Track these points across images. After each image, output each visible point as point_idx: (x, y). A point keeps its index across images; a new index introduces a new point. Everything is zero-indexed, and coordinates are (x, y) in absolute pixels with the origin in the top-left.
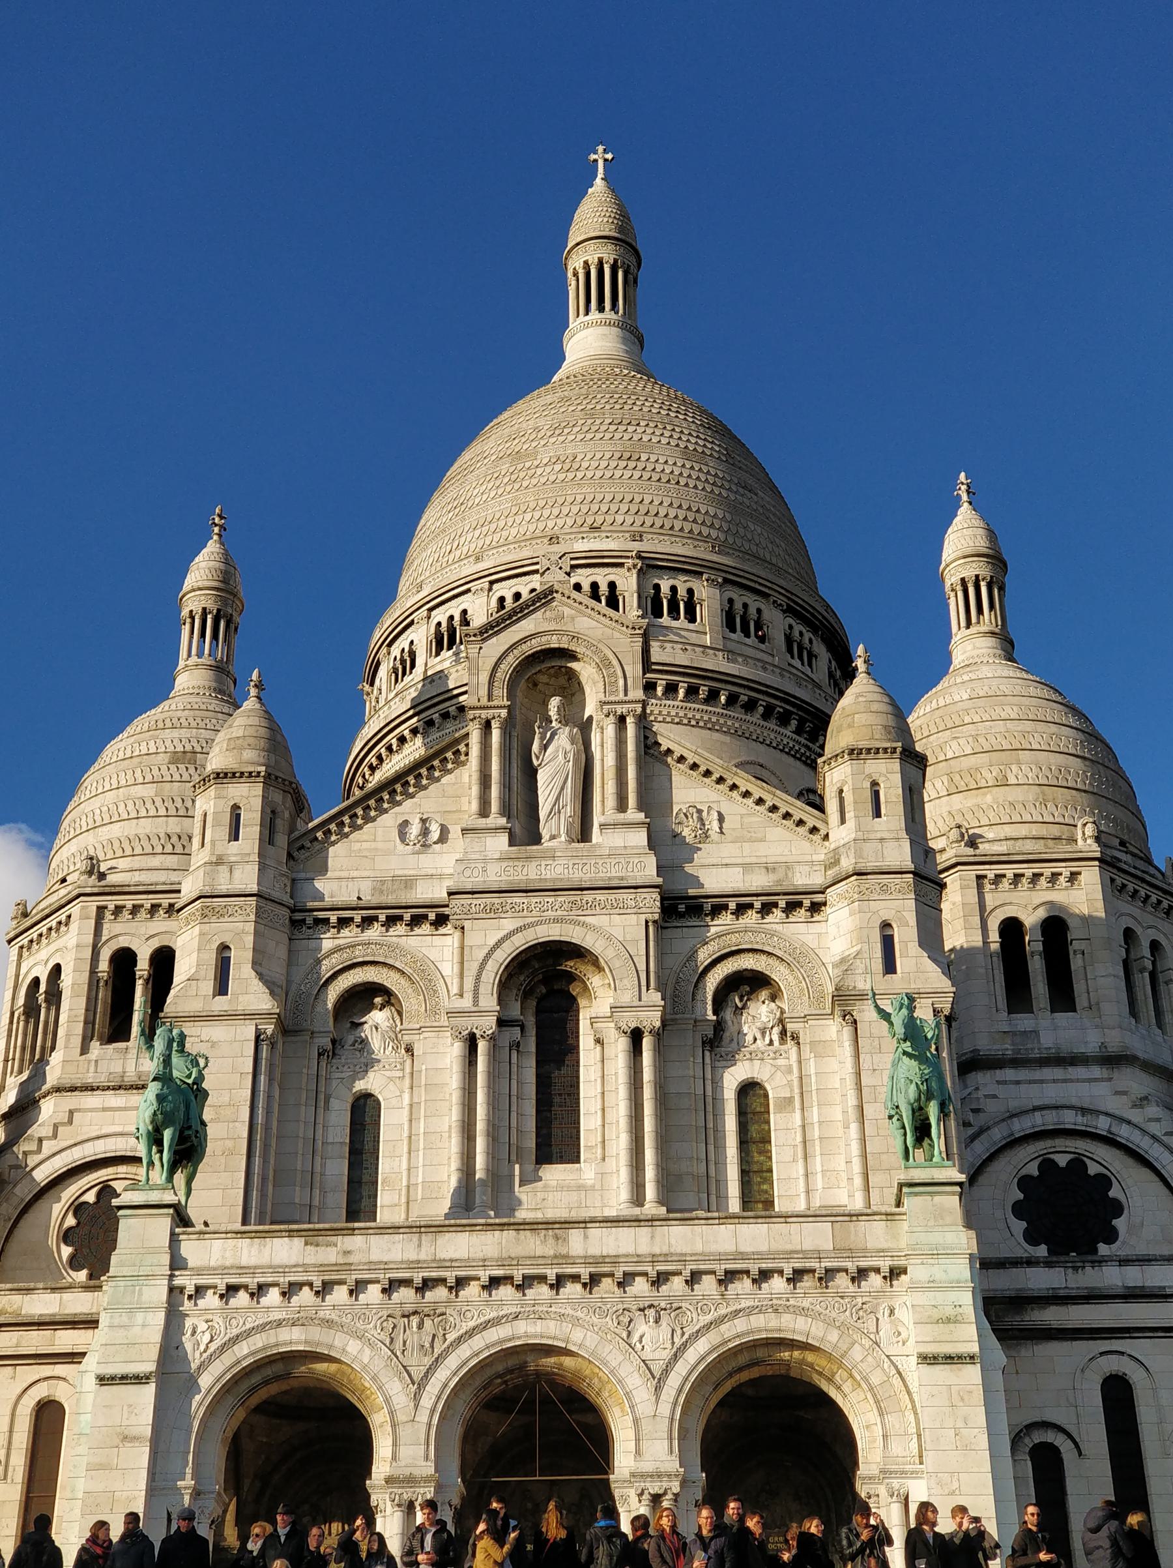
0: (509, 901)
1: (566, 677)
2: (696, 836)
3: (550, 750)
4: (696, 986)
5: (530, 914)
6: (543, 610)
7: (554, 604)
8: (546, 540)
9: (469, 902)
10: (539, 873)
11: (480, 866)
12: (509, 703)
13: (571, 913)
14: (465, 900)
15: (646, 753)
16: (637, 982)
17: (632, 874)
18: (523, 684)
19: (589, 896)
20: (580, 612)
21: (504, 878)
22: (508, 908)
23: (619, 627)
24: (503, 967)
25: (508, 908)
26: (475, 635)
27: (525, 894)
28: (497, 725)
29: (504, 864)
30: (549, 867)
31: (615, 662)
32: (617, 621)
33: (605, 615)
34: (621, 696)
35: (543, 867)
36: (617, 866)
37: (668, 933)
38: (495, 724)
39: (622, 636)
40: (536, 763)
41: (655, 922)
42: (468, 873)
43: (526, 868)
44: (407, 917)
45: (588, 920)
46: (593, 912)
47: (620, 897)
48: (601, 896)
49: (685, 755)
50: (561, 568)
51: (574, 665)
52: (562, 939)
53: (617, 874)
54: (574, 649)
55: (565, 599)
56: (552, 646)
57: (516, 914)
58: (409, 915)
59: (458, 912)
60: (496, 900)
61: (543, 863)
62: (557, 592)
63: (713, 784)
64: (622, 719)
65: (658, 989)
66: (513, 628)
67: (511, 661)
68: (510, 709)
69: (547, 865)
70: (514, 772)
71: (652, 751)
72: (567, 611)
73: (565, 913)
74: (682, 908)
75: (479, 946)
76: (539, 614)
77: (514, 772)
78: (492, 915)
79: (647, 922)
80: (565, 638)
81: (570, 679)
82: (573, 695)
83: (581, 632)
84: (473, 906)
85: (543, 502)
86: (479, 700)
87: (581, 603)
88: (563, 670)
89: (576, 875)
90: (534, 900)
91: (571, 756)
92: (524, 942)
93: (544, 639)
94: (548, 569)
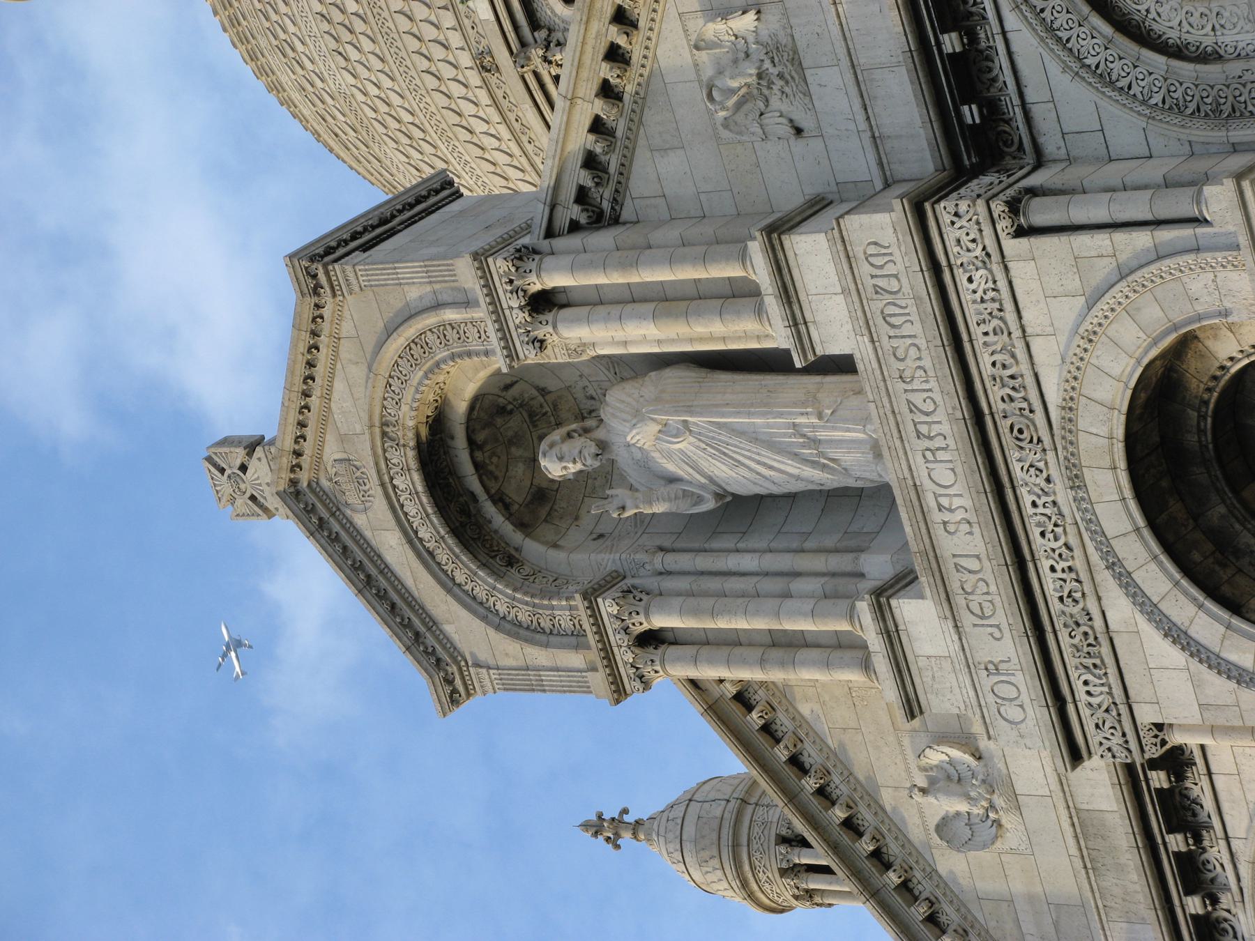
0: (1056, 606)
1: (499, 421)
2: (781, 76)
3: (671, 467)
4: (1176, 52)
5: (1078, 552)
6: (348, 512)
7: (325, 483)
8: (493, 80)
9: (1085, 712)
10: (965, 527)
11: (986, 682)
12: (578, 596)
13: (1044, 433)
14: (1085, 717)
15: (616, 221)
16: (1190, 258)
17: (904, 281)
18: (532, 549)
19: (993, 396)
20: (325, 420)
21: (1000, 618)
22: (1076, 610)
23: (326, 327)
24: (1236, 622)
25: (1076, 610)
26: (450, 682)
27: (1030, 565)
28: (642, 618)
29: (967, 620)
30: (945, 502)
31: (410, 331)
32: (315, 334)
33: (311, 365)
34: (481, 313)
35: (947, 516)
36: (893, 320)
37: (1051, 144)
38: (643, 624)
39: (346, 314)
40: (710, 504)
41: (1014, 207)
42: (1013, 712)
43: (964, 562)
44: (1176, 842)
45: (1054, 397)
46: (1029, 381)
47: (971, 310)
48: (983, 362)
49: (587, 123)
50: (243, 468)
51: (461, 407)
52: (1122, 464)
53: (914, 317)
54: (411, 435)
55: (305, 461)
56: (420, 488)
57: (1088, 588)
58: (1170, 838)
59: (1117, 740)
60: (1065, 643)
61: (937, 517)
62: (294, 483)
63: (639, 37)
64: (542, 303)
65: (1197, 183)
66: (409, 582)
67: (482, 584)
68: (591, 595)
69: (940, 508)
70: (748, 562)
71: (606, 205)
72: (332, 452)
73: (1050, 456)
74: (971, 113)
75: (1197, 684)
76: (360, 520)
77: (748, 562)
78: (1105, 650)
79: (1020, 232)
80: (395, 457)
81: (502, 411)
82: (543, 391)
83: (365, 416)
84: (1095, 701)
85: (429, 79)
86: (594, 669)
87: (302, 425)
88: (480, 437)
89: (945, 428)
90: (1037, 541)
91: (674, 420)
92: (1153, 566)
93: (411, 508)
94: (253, 498)
